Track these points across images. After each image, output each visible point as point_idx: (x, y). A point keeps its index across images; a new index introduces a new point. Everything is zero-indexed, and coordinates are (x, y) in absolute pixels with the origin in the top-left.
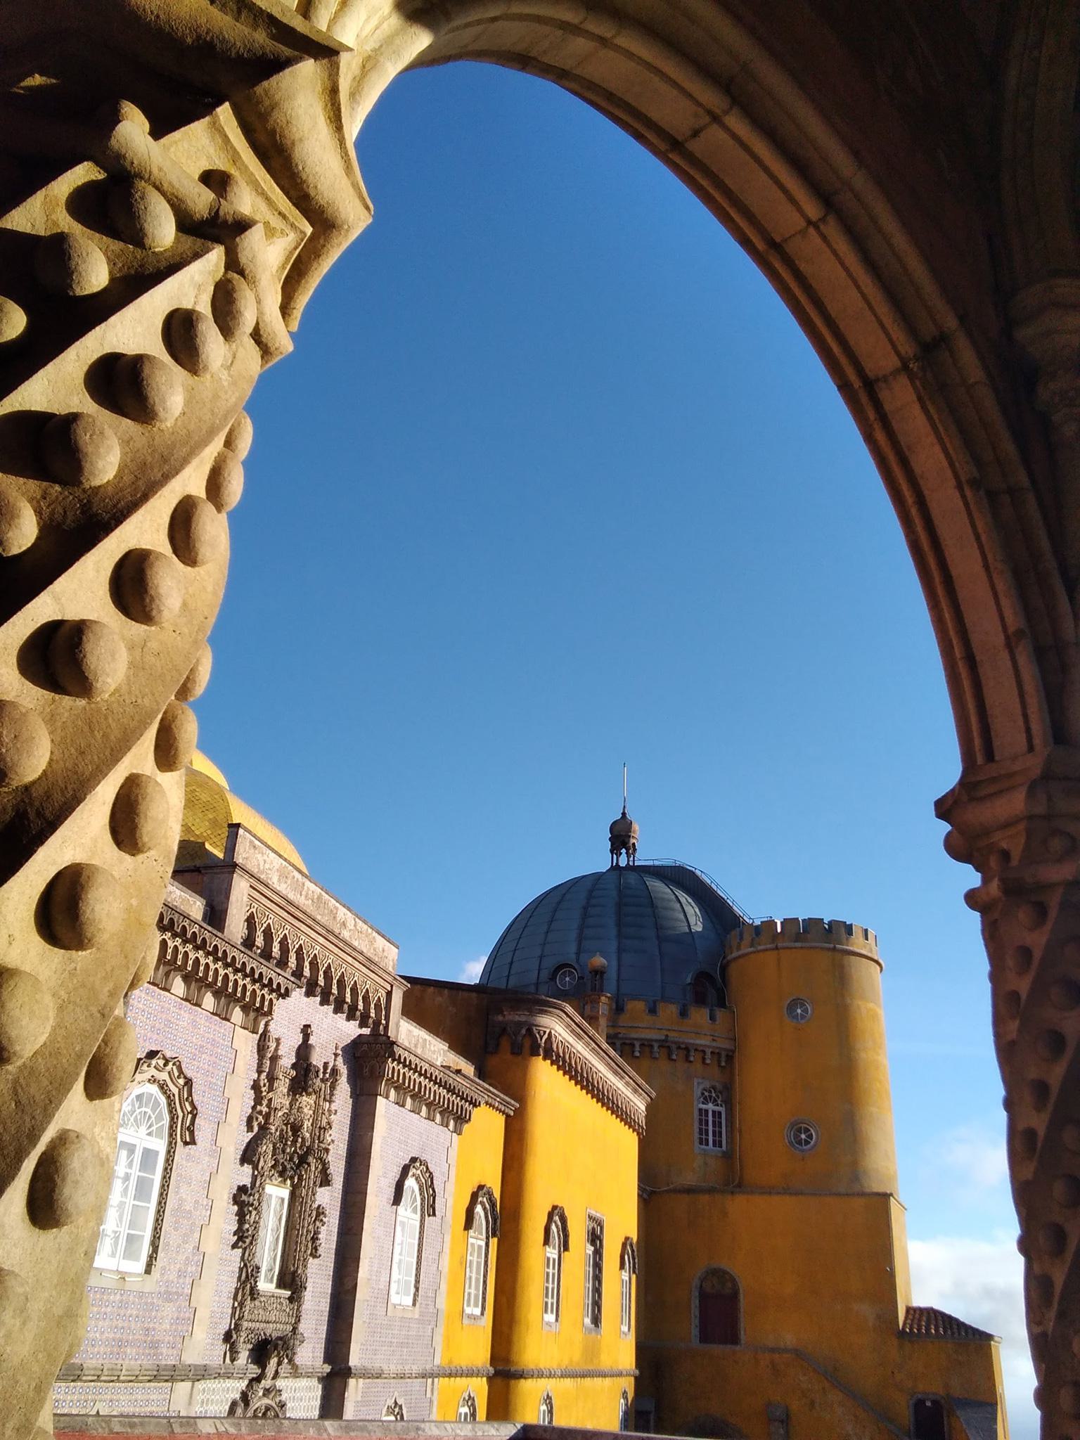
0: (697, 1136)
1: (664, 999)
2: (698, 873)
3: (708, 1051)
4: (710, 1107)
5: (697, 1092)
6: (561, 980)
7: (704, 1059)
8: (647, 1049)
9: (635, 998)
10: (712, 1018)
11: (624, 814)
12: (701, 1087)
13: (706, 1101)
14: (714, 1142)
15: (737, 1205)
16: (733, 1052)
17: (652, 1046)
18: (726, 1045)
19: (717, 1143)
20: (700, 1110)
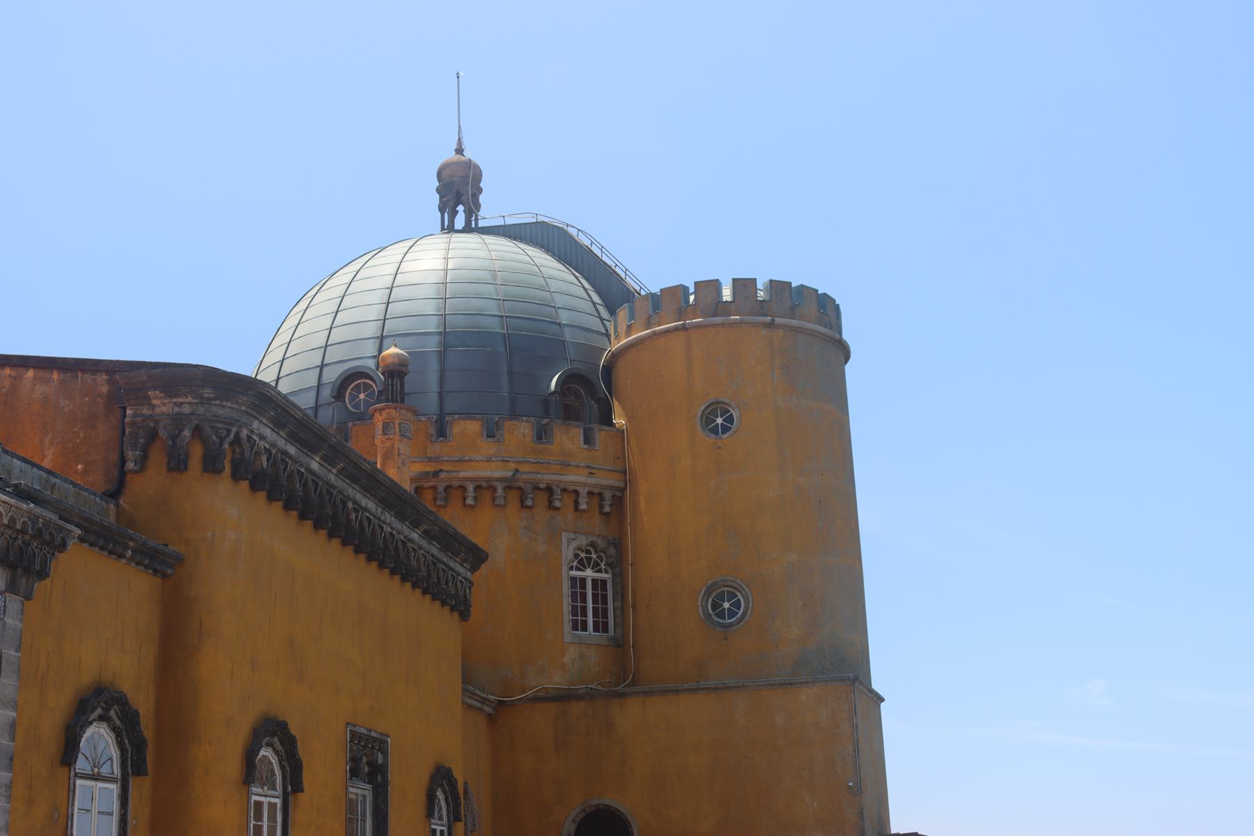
0: (567, 616)
1: (514, 415)
2: (570, 230)
3: (583, 491)
4: (589, 573)
5: (568, 552)
6: (353, 397)
7: (577, 504)
8: (487, 494)
9: (467, 415)
10: (587, 440)
11: (459, 151)
12: (574, 545)
13: (582, 565)
14: (595, 624)
15: (630, 715)
16: (623, 490)
17: (494, 489)
18: (614, 481)
19: (600, 627)
20: (573, 579)
